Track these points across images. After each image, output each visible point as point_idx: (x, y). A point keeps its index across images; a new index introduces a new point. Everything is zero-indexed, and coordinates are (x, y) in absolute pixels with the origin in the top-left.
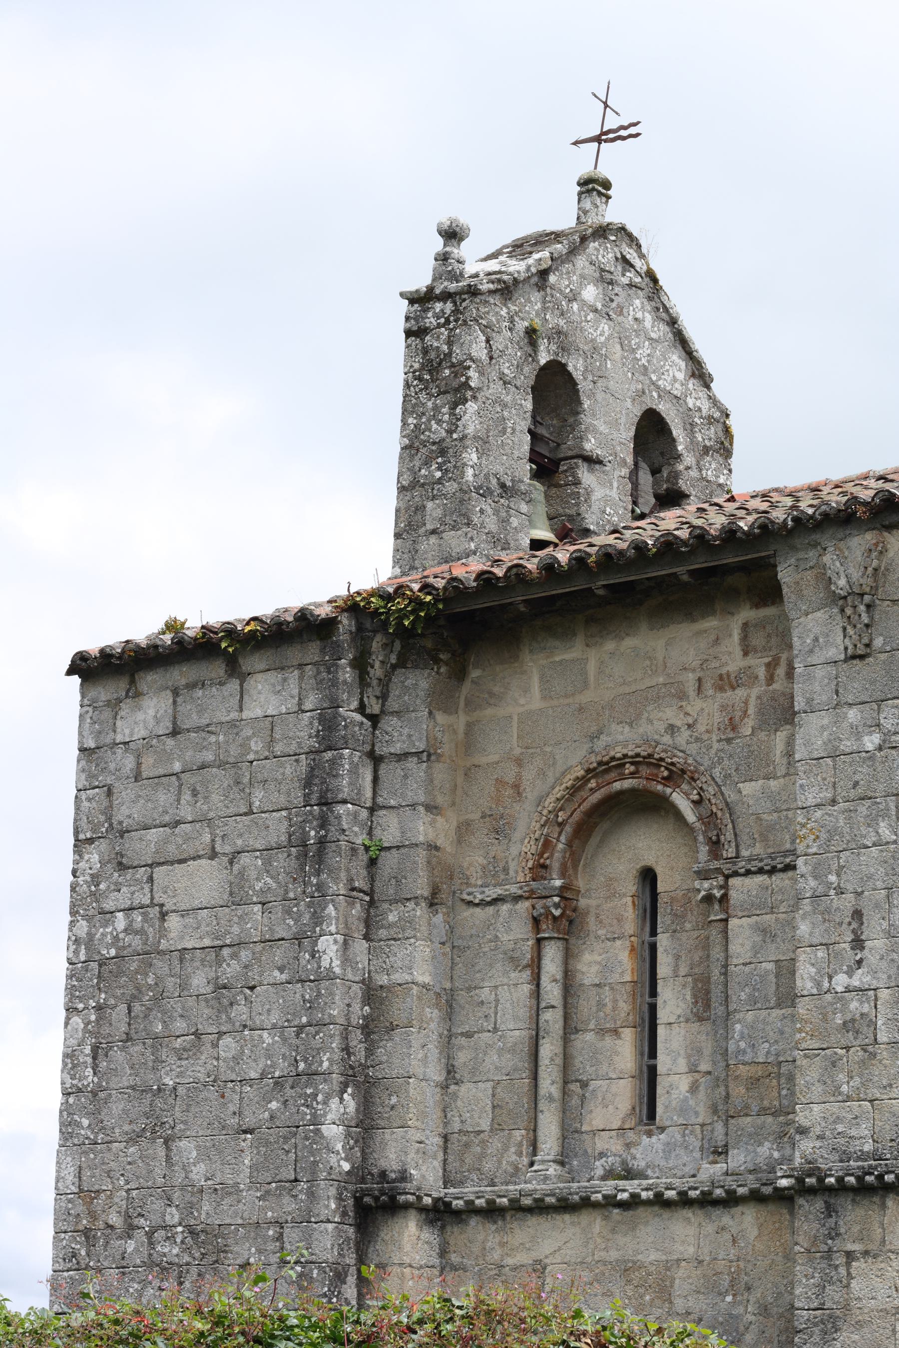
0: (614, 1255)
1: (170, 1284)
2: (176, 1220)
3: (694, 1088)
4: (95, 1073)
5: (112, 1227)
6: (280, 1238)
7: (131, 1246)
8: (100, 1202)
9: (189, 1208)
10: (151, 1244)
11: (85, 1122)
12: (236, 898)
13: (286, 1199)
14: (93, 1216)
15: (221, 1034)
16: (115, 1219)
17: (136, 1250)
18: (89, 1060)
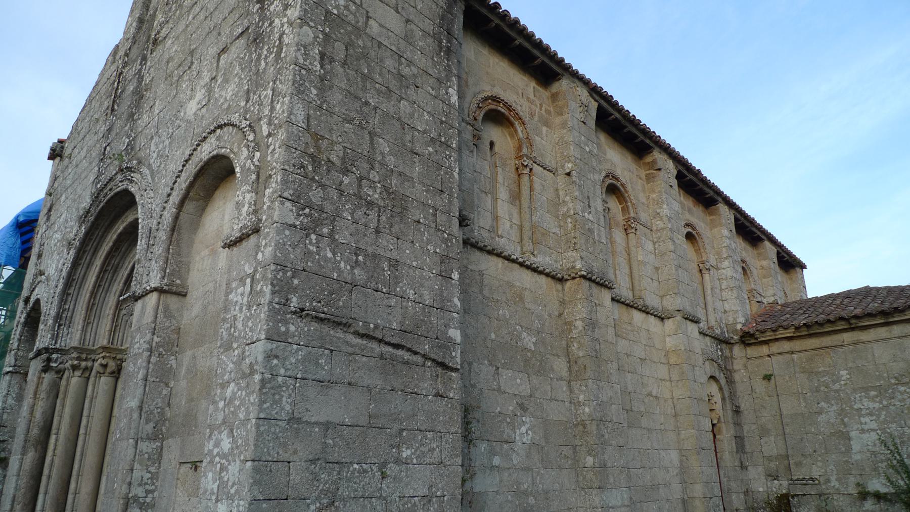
0: (506, 279)
1: (373, 214)
2: (377, 179)
3: (511, 227)
4: (322, 67)
5: (333, 163)
6: (435, 215)
7: (346, 180)
8: (324, 144)
9: (384, 178)
10: (360, 186)
11: (314, 92)
12: (408, 38)
13: (438, 198)
14: (318, 147)
15: (402, 98)
16: (334, 158)
17: (350, 184)
18: (318, 58)
